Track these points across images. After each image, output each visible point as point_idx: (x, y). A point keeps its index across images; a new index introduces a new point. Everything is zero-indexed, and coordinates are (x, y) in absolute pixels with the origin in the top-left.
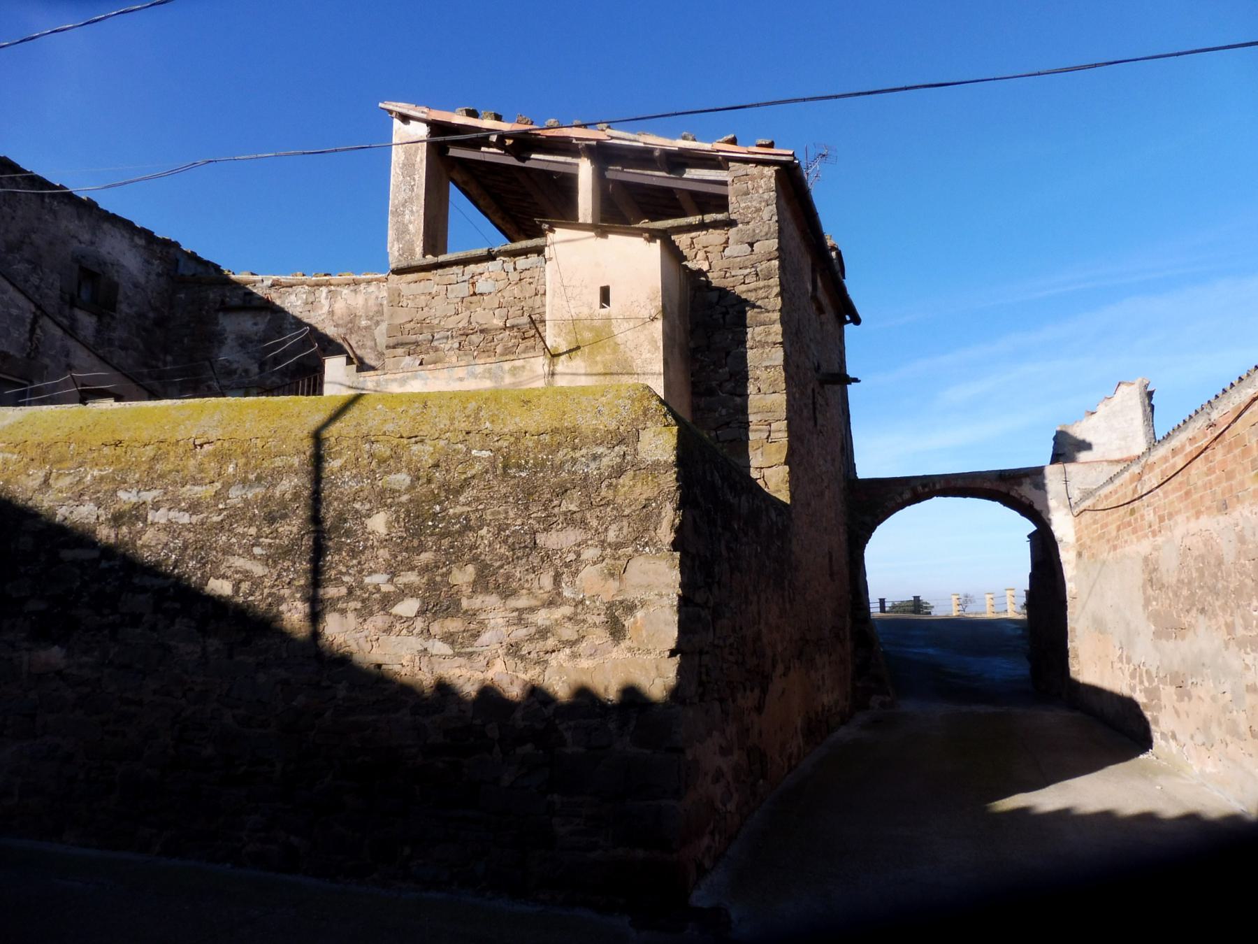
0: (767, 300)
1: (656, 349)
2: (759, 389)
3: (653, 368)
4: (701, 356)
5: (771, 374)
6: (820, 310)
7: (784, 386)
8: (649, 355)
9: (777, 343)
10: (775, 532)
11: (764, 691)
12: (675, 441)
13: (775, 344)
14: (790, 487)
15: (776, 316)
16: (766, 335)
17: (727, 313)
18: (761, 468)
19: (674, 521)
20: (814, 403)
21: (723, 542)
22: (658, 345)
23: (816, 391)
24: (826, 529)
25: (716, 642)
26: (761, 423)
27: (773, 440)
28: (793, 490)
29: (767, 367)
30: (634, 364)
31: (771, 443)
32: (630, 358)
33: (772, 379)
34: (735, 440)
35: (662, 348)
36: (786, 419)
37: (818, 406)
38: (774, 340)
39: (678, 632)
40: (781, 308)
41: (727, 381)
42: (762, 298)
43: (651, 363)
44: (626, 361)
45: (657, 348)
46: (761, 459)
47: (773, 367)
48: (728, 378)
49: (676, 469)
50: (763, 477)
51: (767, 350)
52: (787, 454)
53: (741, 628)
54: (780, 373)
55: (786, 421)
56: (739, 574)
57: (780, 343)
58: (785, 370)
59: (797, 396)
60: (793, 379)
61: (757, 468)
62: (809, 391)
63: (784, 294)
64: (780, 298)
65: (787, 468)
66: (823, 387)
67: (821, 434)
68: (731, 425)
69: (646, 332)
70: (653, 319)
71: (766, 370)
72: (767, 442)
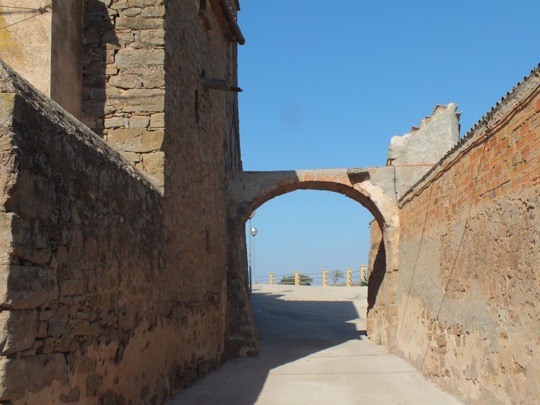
0: (152, 7)
1: (45, 39)
2: (142, 84)
3: (42, 56)
4: (93, 52)
5: (153, 71)
6: (207, 26)
7: (163, 82)
8: (38, 44)
9: (160, 45)
10: (144, 207)
11: (123, 343)
12: (12, 107)
13: (158, 46)
14: (164, 171)
15: (160, 22)
16: (150, 38)
17: (118, 15)
18: (141, 153)
19: (8, 182)
20: (197, 104)
21: (75, 210)
22: (47, 35)
23: (199, 93)
24: (204, 210)
25: (62, 300)
26: (142, 114)
27: (152, 129)
28: (169, 174)
29: (149, 66)
30: (24, 51)
31: (150, 131)
32: (20, 45)
33: (154, 76)
34: (118, 127)
35: (50, 38)
36: (164, 111)
37: (201, 106)
38: (157, 42)
39: (8, 287)
40: (165, 15)
41: (115, 75)
42: (148, 6)
43: (39, 51)
44: (16, 47)
45: (46, 38)
46: (141, 145)
47: (156, 65)
48: (116, 73)
49: (12, 134)
50: (142, 161)
51: (151, 51)
52: (163, 142)
53: (95, 289)
54: (160, 71)
55: (164, 113)
56: (95, 241)
57: (162, 45)
58: (166, 69)
59: (178, 93)
60: (174, 77)
61: (137, 153)
62: (193, 93)
63: (169, 4)
64: (164, 6)
65: (162, 154)
66: (207, 91)
67: (203, 131)
68: (116, 114)
69: (36, 23)
70: (42, 11)
71: (149, 68)
72: (147, 130)
